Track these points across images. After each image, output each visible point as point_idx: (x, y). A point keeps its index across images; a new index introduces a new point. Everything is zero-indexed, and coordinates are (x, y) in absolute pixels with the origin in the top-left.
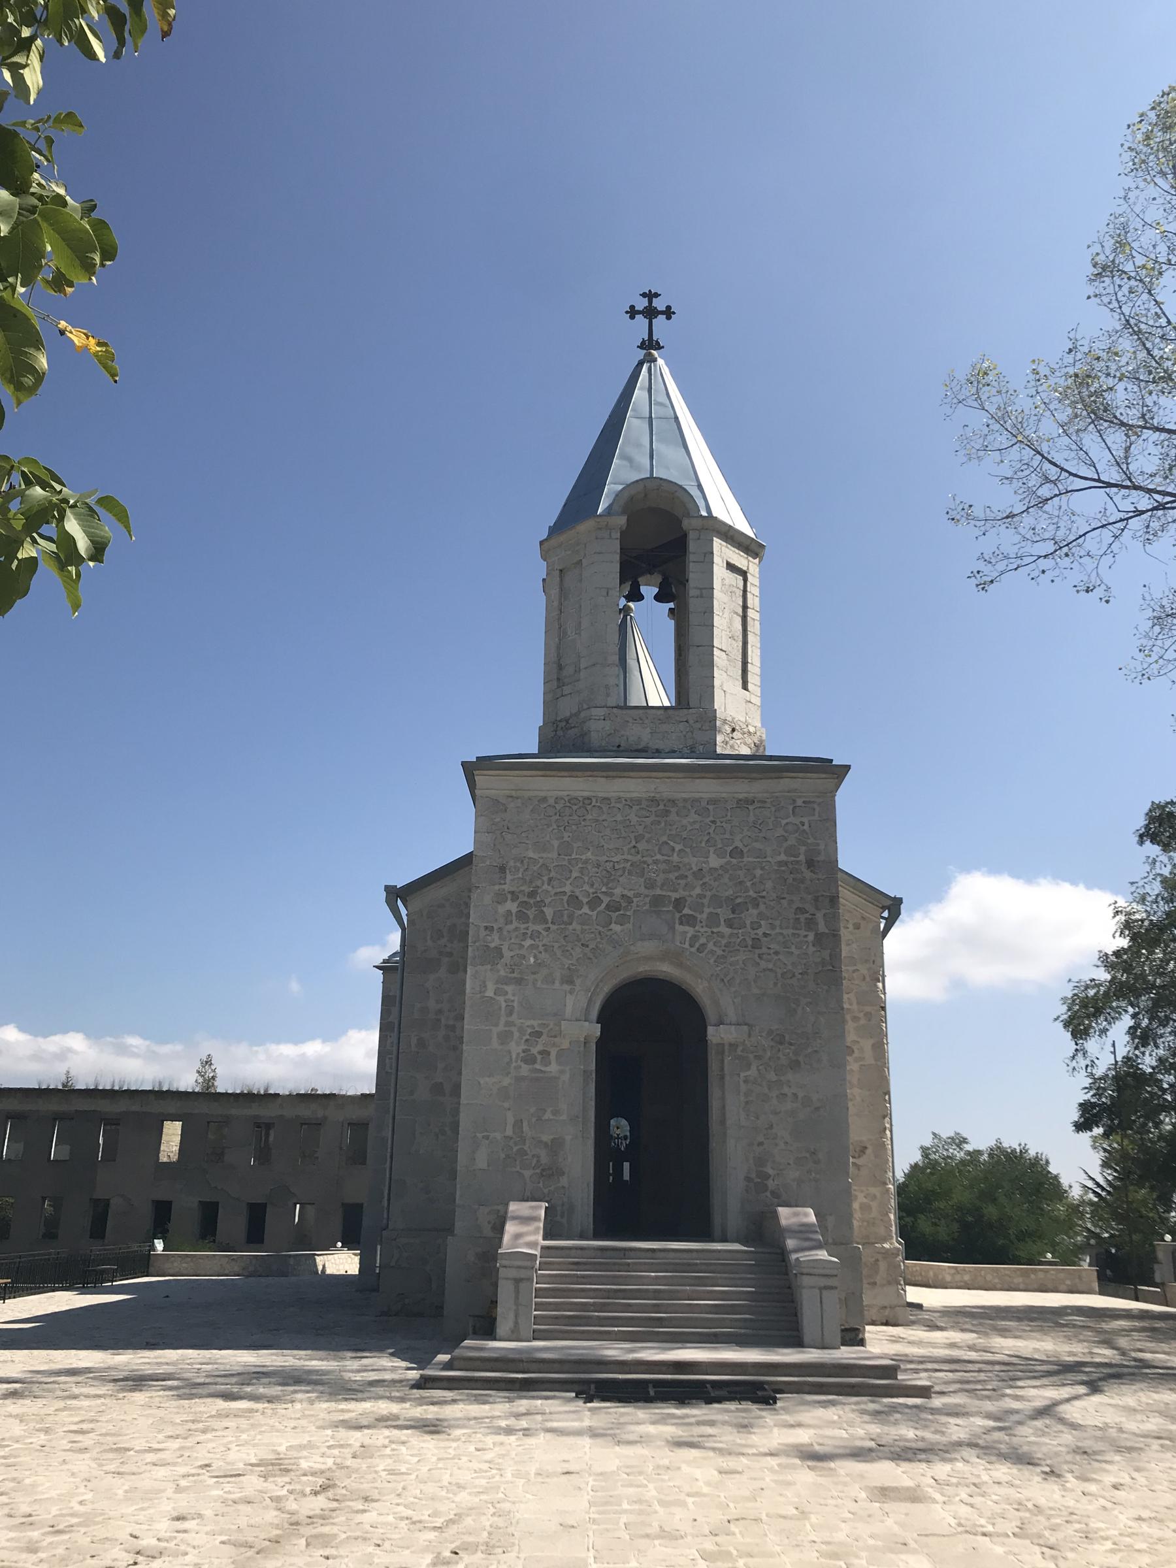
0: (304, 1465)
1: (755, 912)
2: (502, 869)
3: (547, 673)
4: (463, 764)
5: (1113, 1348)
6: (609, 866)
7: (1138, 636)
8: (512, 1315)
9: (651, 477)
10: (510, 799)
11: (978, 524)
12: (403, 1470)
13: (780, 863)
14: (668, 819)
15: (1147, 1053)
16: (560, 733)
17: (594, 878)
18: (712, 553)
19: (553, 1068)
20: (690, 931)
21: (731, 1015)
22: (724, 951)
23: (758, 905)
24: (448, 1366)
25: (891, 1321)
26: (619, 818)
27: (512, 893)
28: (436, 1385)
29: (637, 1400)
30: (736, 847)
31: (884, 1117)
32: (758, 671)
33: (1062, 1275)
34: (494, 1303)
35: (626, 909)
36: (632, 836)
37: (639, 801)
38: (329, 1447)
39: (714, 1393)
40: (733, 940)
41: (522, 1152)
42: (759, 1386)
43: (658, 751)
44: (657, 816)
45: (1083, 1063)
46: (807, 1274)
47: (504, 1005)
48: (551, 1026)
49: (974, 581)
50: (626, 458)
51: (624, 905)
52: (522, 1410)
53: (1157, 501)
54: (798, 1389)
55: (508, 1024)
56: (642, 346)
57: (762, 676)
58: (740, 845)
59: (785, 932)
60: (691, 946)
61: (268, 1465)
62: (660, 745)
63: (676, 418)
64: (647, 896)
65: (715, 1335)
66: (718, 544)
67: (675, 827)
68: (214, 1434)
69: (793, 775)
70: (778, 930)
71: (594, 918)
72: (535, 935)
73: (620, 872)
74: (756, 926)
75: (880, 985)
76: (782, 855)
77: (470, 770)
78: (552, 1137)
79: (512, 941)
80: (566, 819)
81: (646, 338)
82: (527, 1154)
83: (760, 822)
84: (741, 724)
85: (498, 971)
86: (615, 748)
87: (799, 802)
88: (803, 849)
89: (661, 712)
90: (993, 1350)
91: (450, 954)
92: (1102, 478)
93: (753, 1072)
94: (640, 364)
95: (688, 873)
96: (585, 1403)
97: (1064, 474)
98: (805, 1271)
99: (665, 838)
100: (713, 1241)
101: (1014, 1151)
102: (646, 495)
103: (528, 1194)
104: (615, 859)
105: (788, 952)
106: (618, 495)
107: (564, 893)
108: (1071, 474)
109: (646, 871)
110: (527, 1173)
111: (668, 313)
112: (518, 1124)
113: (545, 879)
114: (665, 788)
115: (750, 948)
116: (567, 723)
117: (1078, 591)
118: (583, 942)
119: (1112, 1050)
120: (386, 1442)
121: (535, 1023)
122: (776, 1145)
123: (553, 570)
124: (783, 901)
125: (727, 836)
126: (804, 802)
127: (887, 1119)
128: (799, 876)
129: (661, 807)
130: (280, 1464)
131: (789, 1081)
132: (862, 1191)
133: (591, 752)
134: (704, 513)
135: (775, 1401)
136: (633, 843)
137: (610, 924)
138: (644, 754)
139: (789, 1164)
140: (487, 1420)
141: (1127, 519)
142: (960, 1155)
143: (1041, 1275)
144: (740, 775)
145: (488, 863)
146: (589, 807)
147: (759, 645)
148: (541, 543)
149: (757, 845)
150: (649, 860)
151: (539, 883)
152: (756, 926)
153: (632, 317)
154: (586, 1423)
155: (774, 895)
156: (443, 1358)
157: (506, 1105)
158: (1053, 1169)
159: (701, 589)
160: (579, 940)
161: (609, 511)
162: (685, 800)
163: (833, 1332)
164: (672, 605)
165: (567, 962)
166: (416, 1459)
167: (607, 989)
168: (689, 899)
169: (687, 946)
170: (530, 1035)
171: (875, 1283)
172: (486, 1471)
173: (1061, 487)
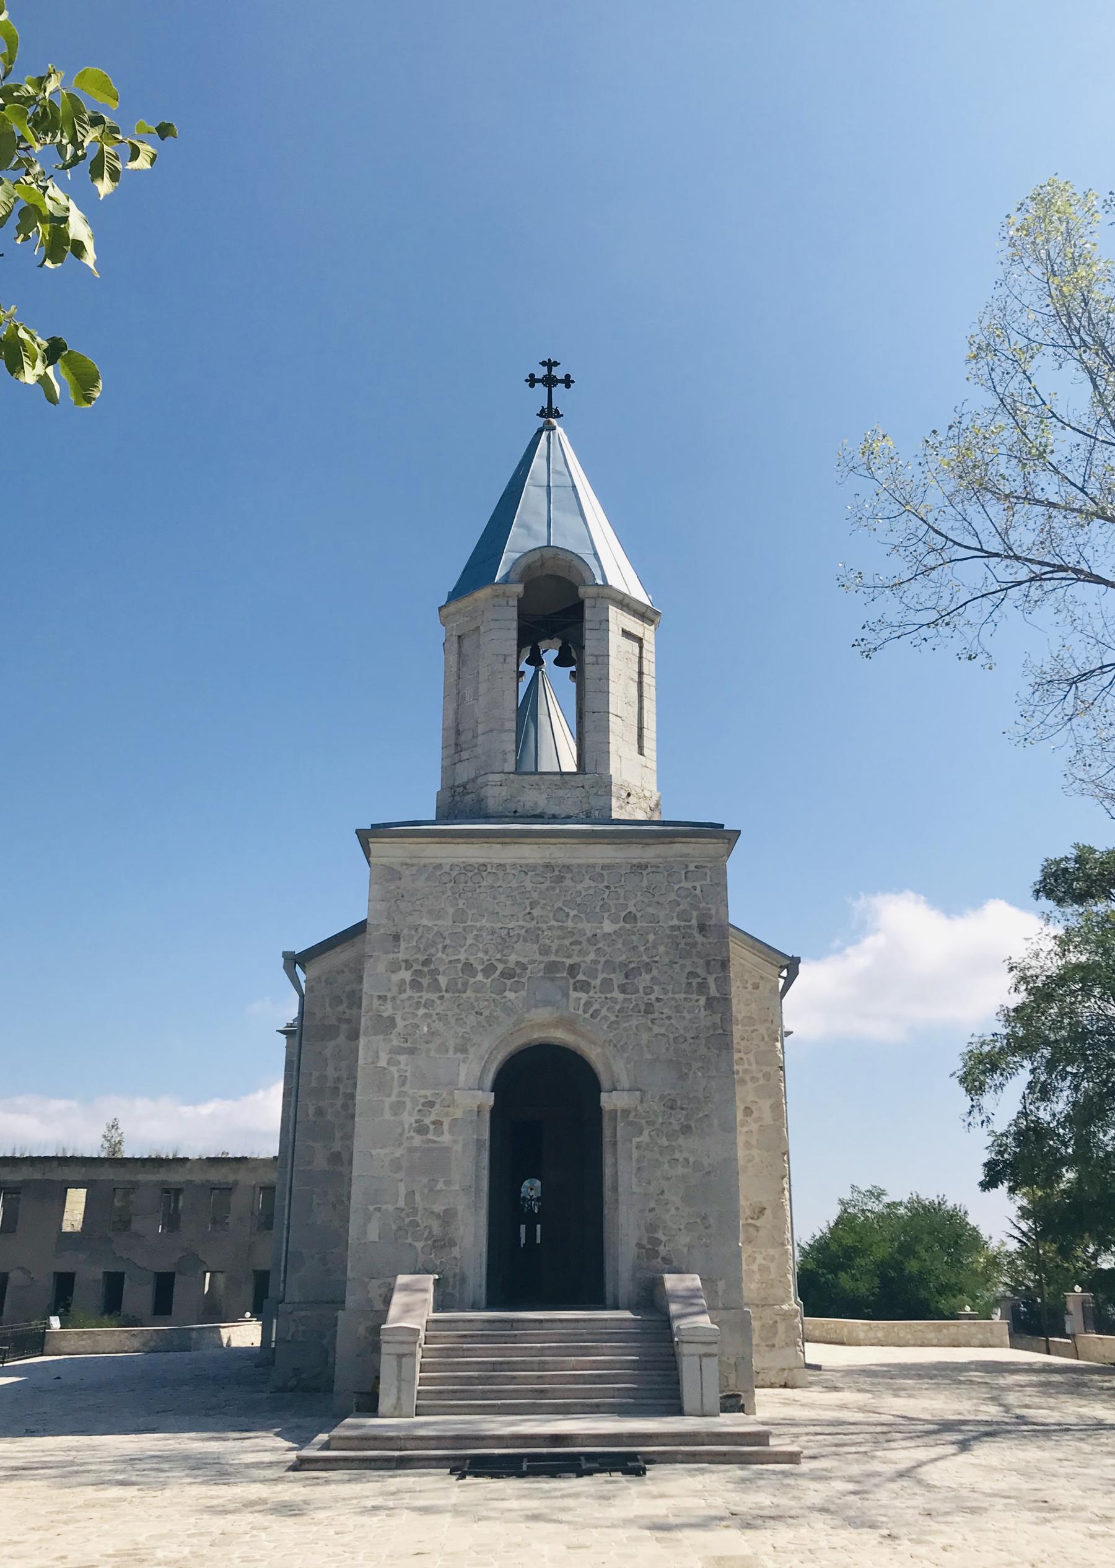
0: (160, 1554)
1: (648, 977)
2: (397, 938)
3: (445, 739)
4: (357, 832)
5: (1000, 1405)
6: (506, 931)
7: (1019, 703)
8: (394, 1391)
9: (549, 546)
10: (405, 867)
11: (866, 590)
12: (258, 1557)
13: (672, 928)
14: (563, 884)
15: (1042, 1108)
16: (457, 798)
17: (488, 946)
18: (608, 621)
19: (446, 1138)
20: (584, 997)
21: (625, 1081)
22: (617, 1016)
23: (651, 970)
24: (326, 1446)
25: (790, 1384)
26: (514, 884)
27: (406, 961)
28: (313, 1466)
29: (509, 1475)
30: (630, 912)
31: (783, 1178)
32: (654, 736)
33: (974, 1330)
34: (378, 1378)
35: (520, 976)
36: (527, 902)
37: (534, 868)
38: (189, 1536)
39: (585, 1466)
40: (626, 1005)
42: (633, 1456)
43: (554, 817)
44: (551, 882)
45: (979, 1119)
46: (687, 1342)
47: (396, 1075)
48: (444, 1096)
49: (857, 649)
50: (524, 526)
51: (518, 971)
52: (393, 1489)
53: (1034, 573)
55: (402, 1094)
56: (541, 414)
57: (659, 740)
58: (632, 909)
59: (677, 996)
60: (585, 1012)
61: (124, 1555)
62: (553, 809)
63: (574, 487)
64: (541, 962)
65: (598, 1405)
66: (613, 611)
67: (570, 892)
68: (76, 1525)
70: (670, 995)
71: (489, 985)
72: (429, 1004)
73: (514, 939)
74: (648, 991)
75: (779, 1045)
76: (675, 919)
77: (365, 837)
78: (443, 1208)
79: (406, 1010)
80: (461, 886)
81: (546, 407)
82: (418, 1226)
83: (653, 886)
84: (637, 789)
85: (391, 1041)
86: (512, 814)
87: (691, 867)
88: (695, 913)
89: (558, 777)
90: (881, 1410)
91: (349, 1021)
92: (985, 548)
93: (644, 1138)
94: (540, 432)
95: (583, 939)
96: (457, 1480)
97: (950, 544)
98: (685, 1339)
99: (559, 904)
100: (605, 1308)
101: (932, 1203)
102: (543, 564)
103: (419, 1266)
104: (510, 926)
105: (680, 1017)
106: (515, 563)
107: (458, 960)
108: (955, 543)
109: (541, 937)
110: (419, 1245)
111: (568, 381)
112: (411, 1194)
113: (440, 946)
114: (558, 853)
115: (642, 1013)
116: (465, 788)
117: (960, 658)
118: (477, 1010)
120: (248, 1528)
121: (428, 1093)
122: (668, 1211)
123: (451, 635)
124: (675, 966)
125: (622, 901)
127: (786, 1179)
128: (690, 941)
129: (557, 873)
130: (136, 1555)
131: (680, 1146)
132: (761, 1253)
133: (487, 818)
134: (600, 582)
135: (644, 1471)
137: (505, 991)
138: (540, 820)
139: (680, 1230)
140: (354, 1502)
141: (1006, 589)
142: (878, 1208)
143: (953, 1330)
144: (633, 840)
145: (382, 931)
146: (484, 874)
147: (654, 710)
148: (440, 609)
149: (650, 910)
150: (545, 927)
151: (433, 951)
152: (648, 991)
153: (532, 386)
154: (453, 1500)
155: (668, 960)
156: (323, 1437)
157: (398, 1176)
158: (972, 1220)
159: (596, 656)
160: (473, 1008)
161: (506, 580)
162: (579, 866)
163: (713, 1398)
164: (573, 668)
165: (461, 1030)
166: (273, 1545)
167: (501, 1056)
168: (583, 965)
169: (581, 1012)
170: (423, 1106)
171: (774, 1346)
172: (339, 1555)
173: (945, 557)
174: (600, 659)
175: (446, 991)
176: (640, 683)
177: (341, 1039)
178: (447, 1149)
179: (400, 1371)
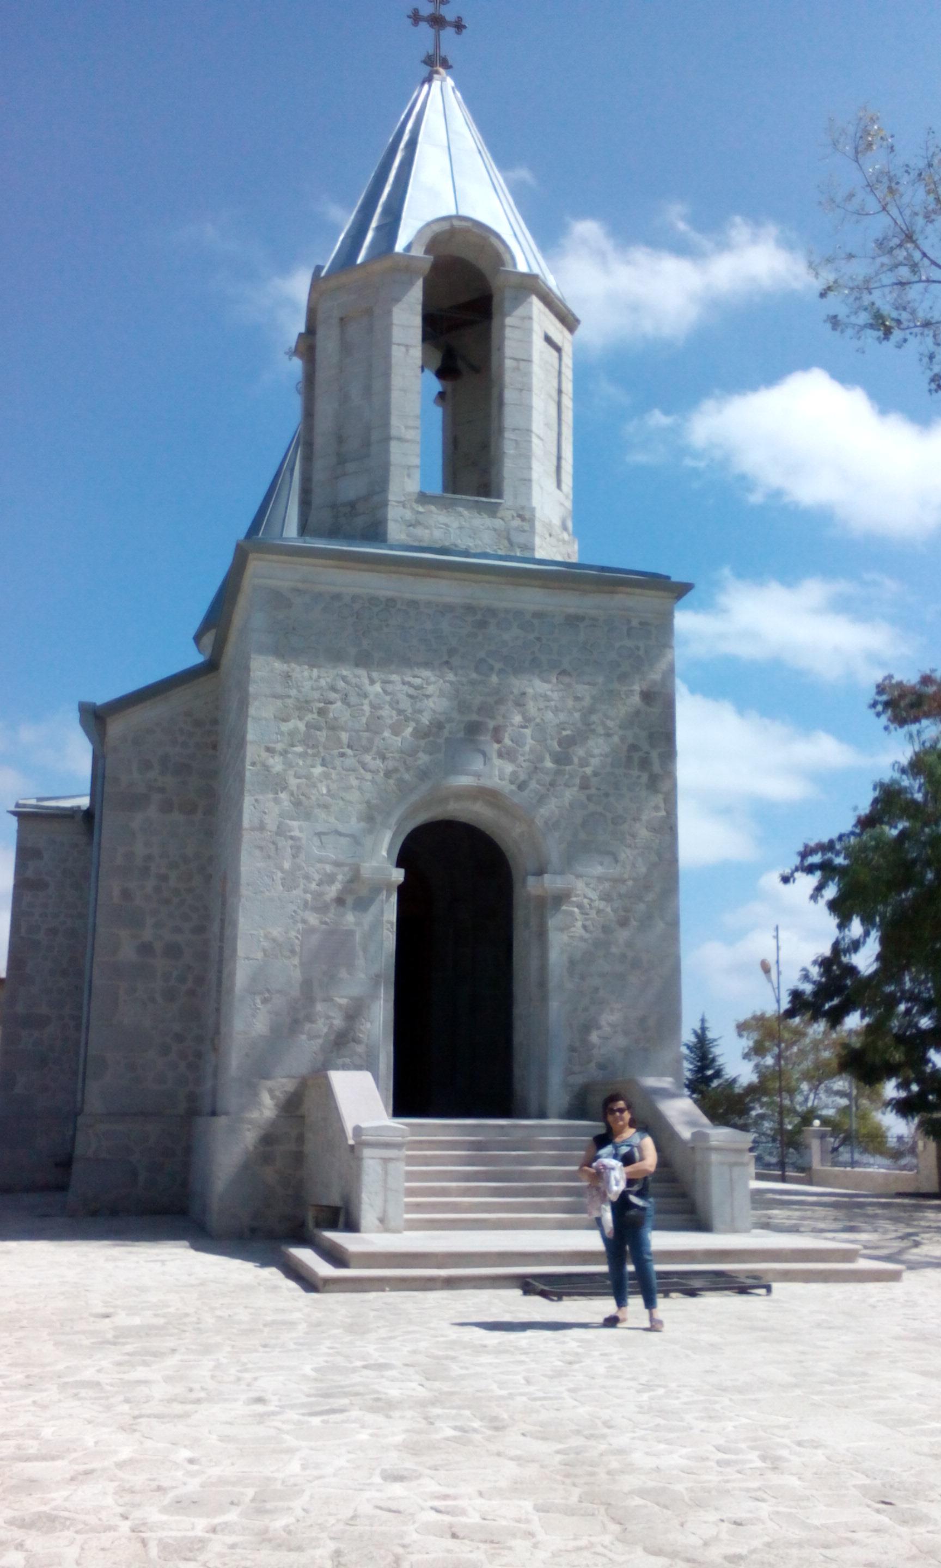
37: (449, 608)
54: (788, 1276)
69: (629, 590)
87: (635, 623)
91: (162, 790)
99: (482, 654)
119: (775, 934)
162: (507, 611)
167: (409, 827)
174: (522, 364)
175: (350, 747)
177: (152, 812)
178: (350, 933)
179: (385, 1181)
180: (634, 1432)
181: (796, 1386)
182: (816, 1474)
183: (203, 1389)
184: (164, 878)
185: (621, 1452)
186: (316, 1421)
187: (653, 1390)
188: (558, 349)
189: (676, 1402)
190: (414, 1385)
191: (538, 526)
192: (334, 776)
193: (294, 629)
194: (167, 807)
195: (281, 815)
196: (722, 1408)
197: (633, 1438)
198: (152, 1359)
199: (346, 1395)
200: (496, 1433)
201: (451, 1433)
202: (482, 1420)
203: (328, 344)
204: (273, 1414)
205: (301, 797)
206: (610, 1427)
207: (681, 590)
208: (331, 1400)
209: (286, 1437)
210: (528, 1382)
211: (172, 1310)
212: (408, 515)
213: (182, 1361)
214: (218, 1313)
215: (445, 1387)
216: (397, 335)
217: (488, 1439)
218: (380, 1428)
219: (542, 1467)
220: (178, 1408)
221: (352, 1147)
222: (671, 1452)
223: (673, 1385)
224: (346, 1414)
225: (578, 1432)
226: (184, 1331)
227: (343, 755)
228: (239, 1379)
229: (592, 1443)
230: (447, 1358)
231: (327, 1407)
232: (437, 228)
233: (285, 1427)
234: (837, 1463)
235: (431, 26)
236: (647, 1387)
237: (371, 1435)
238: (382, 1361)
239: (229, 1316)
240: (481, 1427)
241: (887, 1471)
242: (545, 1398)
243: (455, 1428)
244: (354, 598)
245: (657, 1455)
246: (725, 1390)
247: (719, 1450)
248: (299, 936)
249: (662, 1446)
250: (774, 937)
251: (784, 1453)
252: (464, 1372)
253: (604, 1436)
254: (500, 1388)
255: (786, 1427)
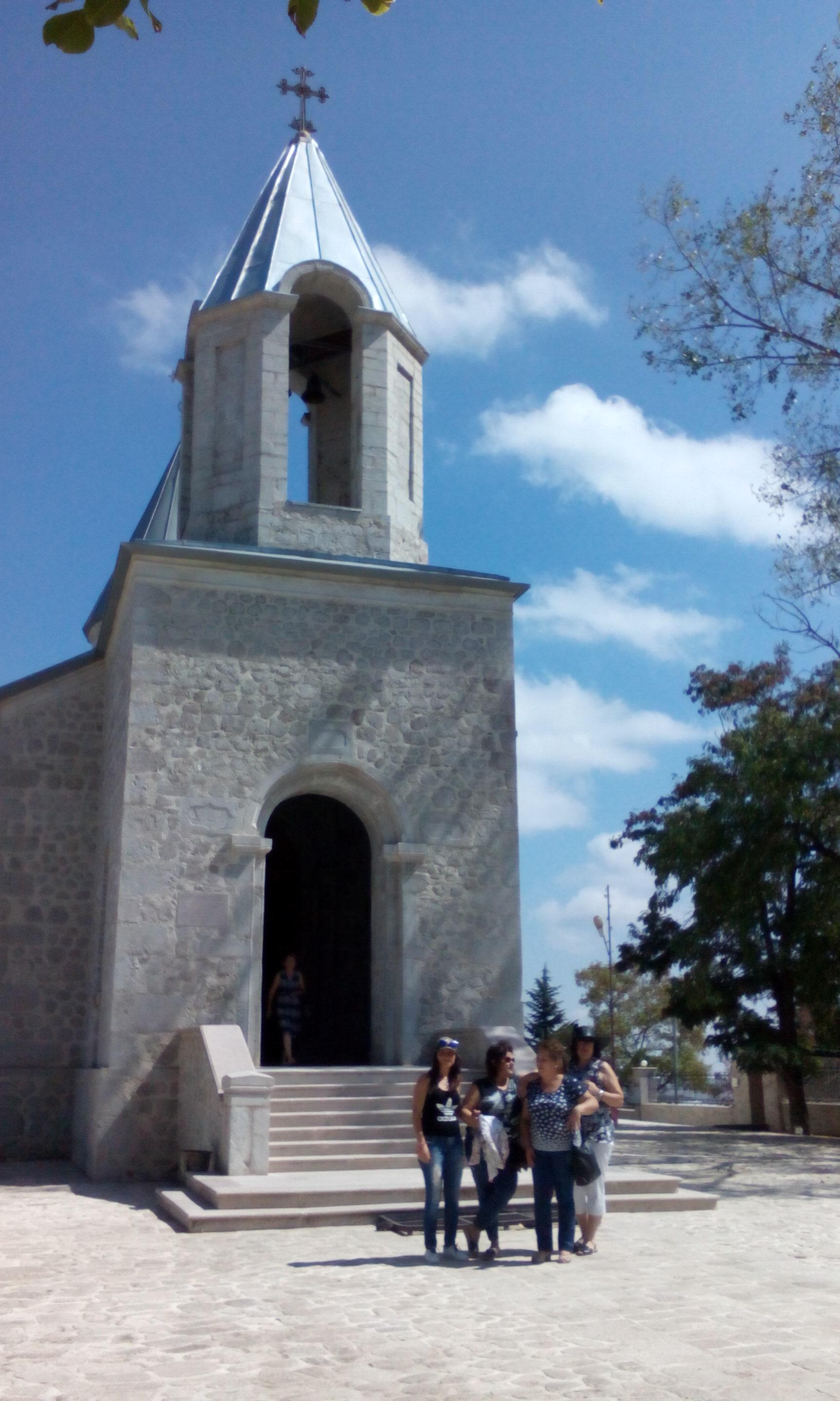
8: (245, 1146)
41: (185, 977)
87: (478, 618)
91: (50, 767)
112: (181, 944)
126: (484, 619)
136: (310, 648)
162: (364, 607)
167: (277, 801)
174: (378, 391)
175: (222, 728)
176: (411, 426)
180: (472, 1360)
181: (620, 1311)
182: (634, 1395)
183: (74, 1328)
184: (51, 848)
185: (459, 1379)
186: (179, 1357)
187: (491, 1319)
188: (410, 378)
189: (511, 1329)
190: (272, 1320)
191: (393, 533)
192: (208, 755)
193: (172, 622)
194: (55, 783)
195: (160, 790)
196: (553, 1334)
197: (471, 1366)
198: (28, 1299)
199: (208, 1331)
200: (345, 1365)
201: (303, 1365)
202: (333, 1351)
203: (205, 371)
204: (140, 1351)
205: (178, 774)
206: (449, 1355)
207: (519, 590)
208: (192, 1337)
209: (150, 1373)
210: (377, 1313)
211: (50, 1252)
212: (277, 521)
213: (56, 1301)
214: (93, 1254)
215: (300, 1320)
216: (267, 363)
217: (338, 1371)
218: (238, 1362)
219: (386, 1396)
220: (49, 1347)
221: (221, 1096)
222: (505, 1378)
223: (509, 1314)
224: (208, 1350)
225: (420, 1362)
226: (60, 1272)
227: (217, 736)
228: (109, 1318)
229: (433, 1371)
230: (304, 1292)
231: (190, 1344)
232: (302, 271)
233: (151, 1364)
234: (654, 1384)
235: (298, 95)
236: (485, 1316)
237: (229, 1369)
238: (244, 1297)
239: (104, 1256)
240: (332, 1358)
241: (698, 1391)
242: (392, 1330)
243: (308, 1361)
244: (228, 595)
245: (491, 1381)
246: (555, 1317)
247: (547, 1375)
248: (176, 902)
249: (496, 1372)
250: (605, 896)
251: (606, 1376)
252: (319, 1306)
253: (443, 1364)
254: (351, 1321)
255: (609, 1351)
